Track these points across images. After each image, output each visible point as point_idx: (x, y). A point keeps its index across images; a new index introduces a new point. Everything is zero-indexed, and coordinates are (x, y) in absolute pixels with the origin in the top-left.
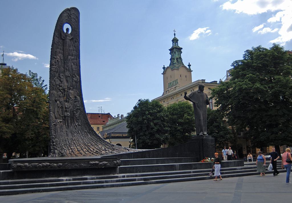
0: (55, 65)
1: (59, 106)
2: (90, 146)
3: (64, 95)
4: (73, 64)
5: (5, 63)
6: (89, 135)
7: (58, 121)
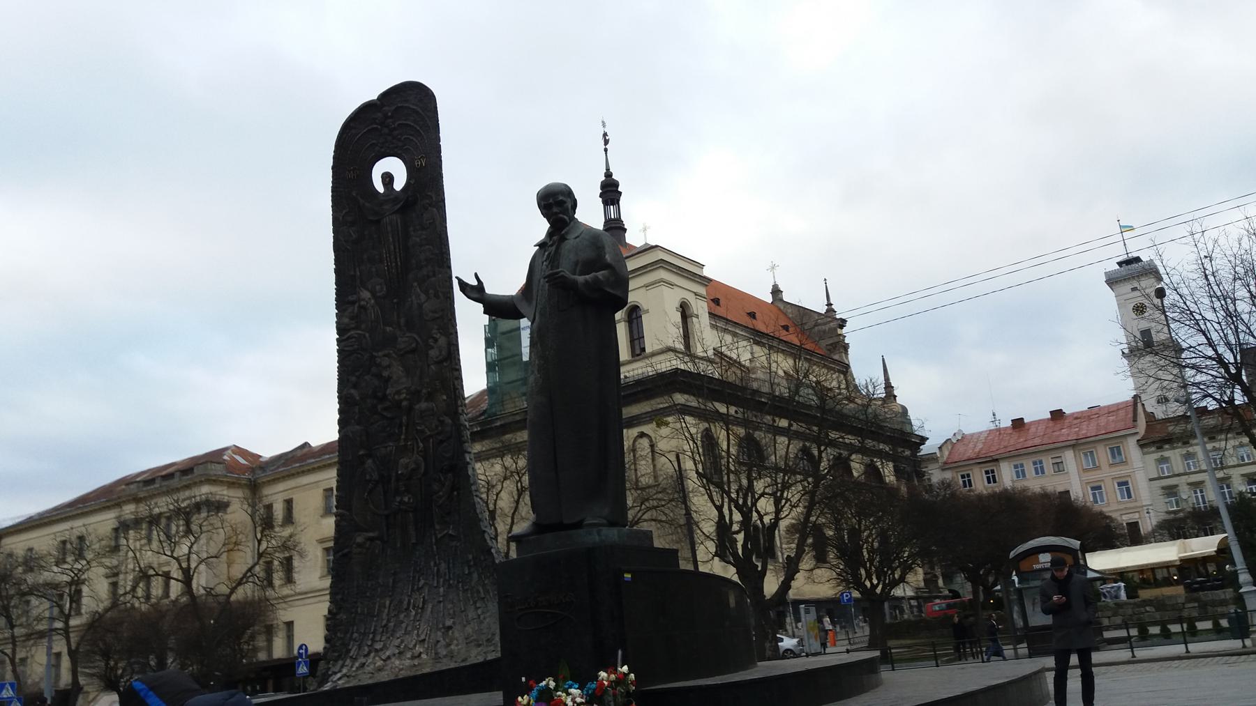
1: (368, 477)
2: (450, 628)
3: (401, 426)
4: (423, 297)
5: (1135, 255)
6: (475, 576)
7: (359, 540)
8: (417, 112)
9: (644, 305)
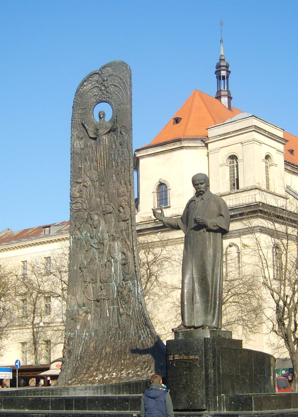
0: (79, 196)
1: (85, 280)
8: (121, 79)
9: (240, 157)
